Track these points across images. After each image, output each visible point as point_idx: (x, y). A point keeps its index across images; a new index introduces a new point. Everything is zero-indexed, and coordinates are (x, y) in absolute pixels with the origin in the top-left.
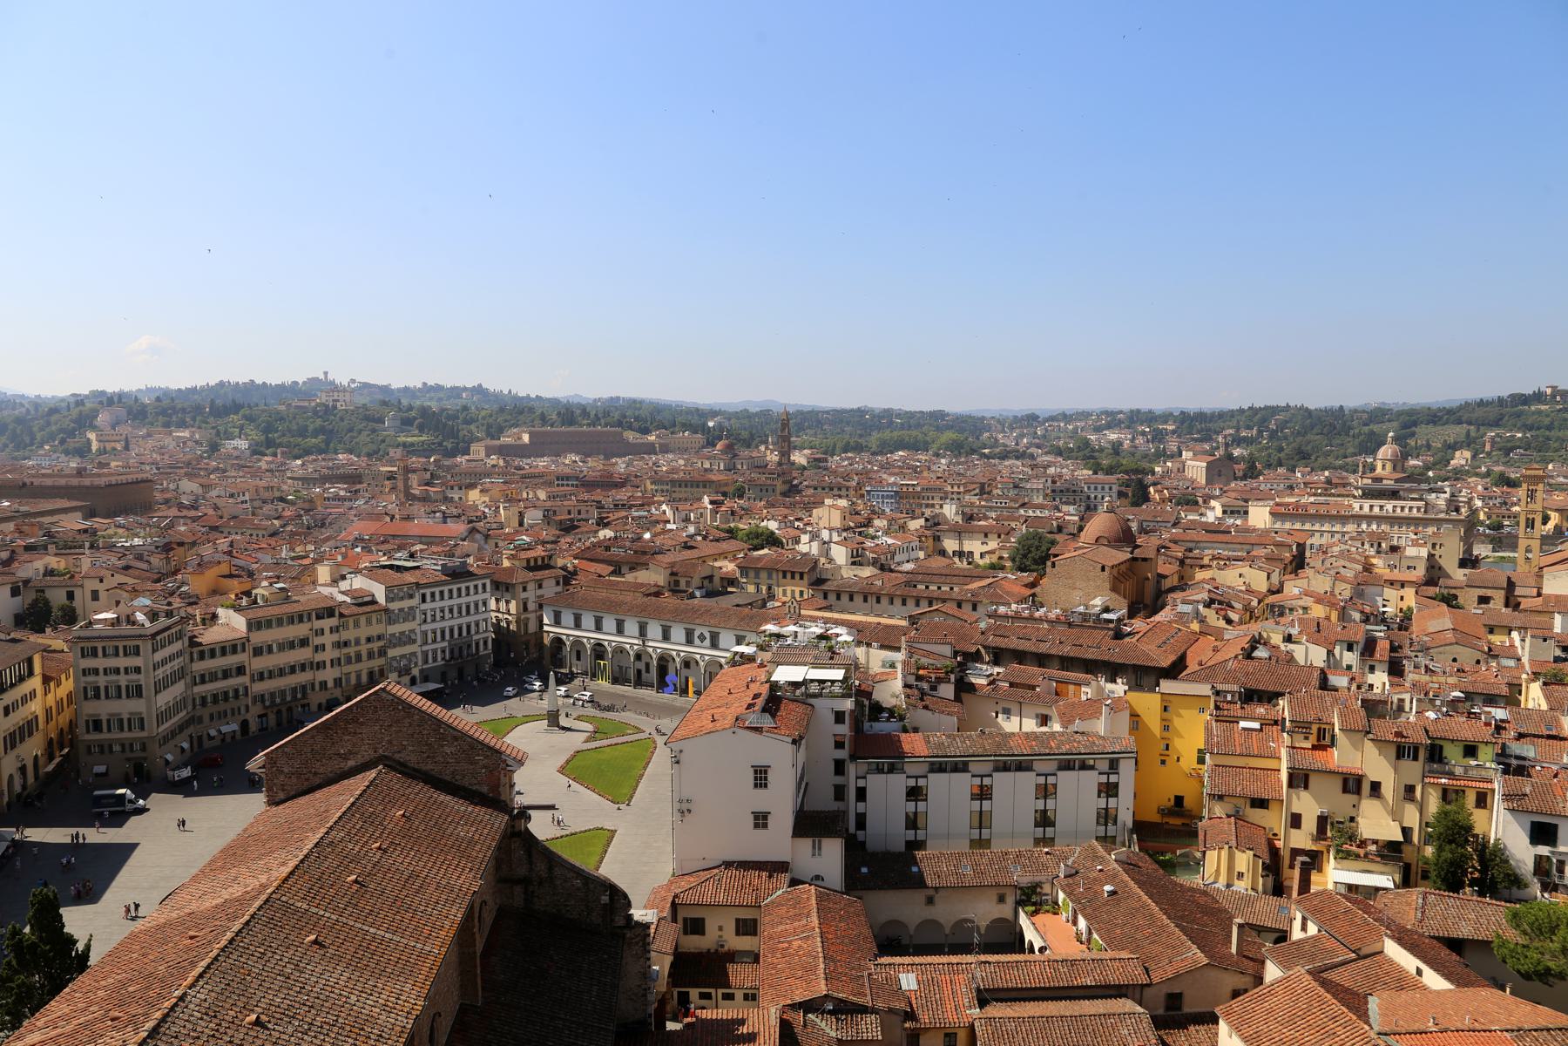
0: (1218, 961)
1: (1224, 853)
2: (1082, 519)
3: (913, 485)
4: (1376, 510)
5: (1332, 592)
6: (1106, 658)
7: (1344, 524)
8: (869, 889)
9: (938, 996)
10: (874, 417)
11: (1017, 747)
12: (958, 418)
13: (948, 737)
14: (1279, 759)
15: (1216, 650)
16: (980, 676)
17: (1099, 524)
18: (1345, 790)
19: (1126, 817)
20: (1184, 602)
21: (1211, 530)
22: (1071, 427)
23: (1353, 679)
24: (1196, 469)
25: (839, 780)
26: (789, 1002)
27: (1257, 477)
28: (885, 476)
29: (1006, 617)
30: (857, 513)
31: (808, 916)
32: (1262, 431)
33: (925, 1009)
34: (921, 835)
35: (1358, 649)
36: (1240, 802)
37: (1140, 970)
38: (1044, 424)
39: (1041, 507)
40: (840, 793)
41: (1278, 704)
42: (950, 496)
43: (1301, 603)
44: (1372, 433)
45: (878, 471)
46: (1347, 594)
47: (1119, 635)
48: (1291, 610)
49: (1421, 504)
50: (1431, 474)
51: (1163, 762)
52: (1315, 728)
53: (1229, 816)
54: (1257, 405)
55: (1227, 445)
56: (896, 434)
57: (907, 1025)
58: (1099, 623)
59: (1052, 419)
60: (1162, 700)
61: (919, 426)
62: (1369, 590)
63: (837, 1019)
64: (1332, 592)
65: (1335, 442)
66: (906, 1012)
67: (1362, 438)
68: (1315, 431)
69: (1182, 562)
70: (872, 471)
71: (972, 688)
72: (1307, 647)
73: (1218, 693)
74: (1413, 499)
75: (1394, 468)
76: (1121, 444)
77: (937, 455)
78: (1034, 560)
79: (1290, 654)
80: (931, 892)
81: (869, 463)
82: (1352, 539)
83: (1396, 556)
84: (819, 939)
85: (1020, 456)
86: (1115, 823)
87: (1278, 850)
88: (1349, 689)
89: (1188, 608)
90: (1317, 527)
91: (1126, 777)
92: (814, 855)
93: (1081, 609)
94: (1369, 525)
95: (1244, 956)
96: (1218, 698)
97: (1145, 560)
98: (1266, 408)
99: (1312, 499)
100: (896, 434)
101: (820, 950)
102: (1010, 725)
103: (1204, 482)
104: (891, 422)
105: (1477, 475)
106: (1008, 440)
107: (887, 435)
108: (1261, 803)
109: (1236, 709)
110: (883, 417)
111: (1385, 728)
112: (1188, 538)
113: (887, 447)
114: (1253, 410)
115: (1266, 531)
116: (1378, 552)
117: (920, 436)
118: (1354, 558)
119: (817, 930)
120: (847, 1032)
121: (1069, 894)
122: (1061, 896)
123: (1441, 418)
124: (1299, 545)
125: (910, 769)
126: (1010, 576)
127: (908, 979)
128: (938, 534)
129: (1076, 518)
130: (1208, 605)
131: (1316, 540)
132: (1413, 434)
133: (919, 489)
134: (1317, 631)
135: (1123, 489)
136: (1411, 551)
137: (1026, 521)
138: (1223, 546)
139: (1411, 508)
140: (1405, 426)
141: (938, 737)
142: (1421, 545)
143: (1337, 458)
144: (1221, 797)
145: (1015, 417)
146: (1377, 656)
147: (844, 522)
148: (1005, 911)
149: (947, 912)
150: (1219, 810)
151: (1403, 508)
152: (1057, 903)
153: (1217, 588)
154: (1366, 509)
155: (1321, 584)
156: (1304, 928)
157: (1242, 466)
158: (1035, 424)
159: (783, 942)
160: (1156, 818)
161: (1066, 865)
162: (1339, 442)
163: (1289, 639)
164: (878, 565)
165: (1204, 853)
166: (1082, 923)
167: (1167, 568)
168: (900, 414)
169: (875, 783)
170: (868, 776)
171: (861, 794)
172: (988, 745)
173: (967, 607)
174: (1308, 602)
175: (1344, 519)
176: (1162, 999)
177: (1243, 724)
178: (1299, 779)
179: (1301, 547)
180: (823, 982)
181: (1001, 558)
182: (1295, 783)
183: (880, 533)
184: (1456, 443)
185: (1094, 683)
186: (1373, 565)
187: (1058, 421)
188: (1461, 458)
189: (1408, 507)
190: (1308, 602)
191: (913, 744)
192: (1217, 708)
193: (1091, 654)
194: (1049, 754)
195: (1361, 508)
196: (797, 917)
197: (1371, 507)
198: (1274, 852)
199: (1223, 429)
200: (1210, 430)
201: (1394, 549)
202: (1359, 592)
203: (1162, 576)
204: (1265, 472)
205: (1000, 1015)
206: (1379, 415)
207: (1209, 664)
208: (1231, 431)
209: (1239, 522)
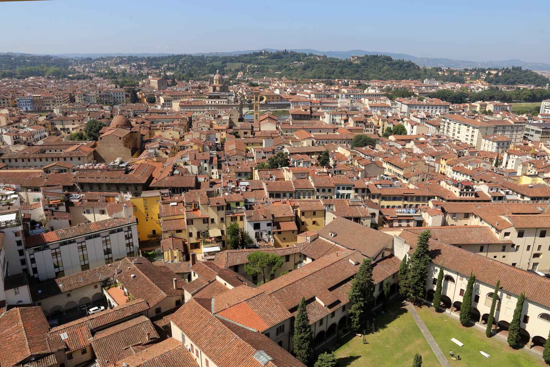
0: (170, 294)
1: (170, 252)
2: (111, 112)
3: (39, 96)
4: (213, 103)
5: (200, 138)
6: (123, 182)
7: (203, 109)
8: (43, 299)
9: (76, 338)
10: (16, 59)
11: (93, 229)
12: (56, 60)
13: (66, 230)
14: (184, 215)
15: (161, 172)
16: (75, 198)
17: (117, 120)
18: (204, 223)
19: (136, 244)
20: (151, 149)
21: (159, 113)
22: (106, 63)
23: (205, 178)
24: (154, 82)
25: (22, 257)
26: (15, 363)
27: (176, 85)
28: (25, 91)
29: (83, 170)
30: (13, 116)
31: (18, 321)
32: (177, 65)
33: (72, 344)
34: (61, 269)
35: (208, 162)
36: (173, 232)
37: (146, 304)
38: (94, 62)
39: (95, 107)
40: (23, 262)
41: (182, 195)
42: (56, 100)
43: (190, 145)
44: (213, 66)
45: (21, 88)
46: (204, 139)
47: (127, 172)
48: (187, 147)
49: (226, 100)
50: (231, 81)
51: (147, 220)
52: (193, 204)
53: (170, 237)
54: (175, 55)
55: (165, 71)
56: (28, 68)
57: (66, 353)
58: (119, 168)
59: (98, 60)
60: (144, 200)
61: (39, 63)
62: (212, 136)
63: (37, 362)
64: (200, 138)
65: (201, 69)
66: (65, 349)
67: (210, 67)
68: (195, 65)
69: (150, 128)
70: (18, 88)
71: (72, 204)
72: (191, 167)
73: (162, 194)
74: (224, 99)
75: (219, 83)
76: (126, 71)
77: (49, 78)
78: (94, 131)
79: (187, 169)
80: (69, 292)
81: (17, 84)
82: (206, 114)
83: (220, 119)
84: (24, 332)
85: (85, 78)
86: (133, 246)
87: (186, 244)
88: (205, 182)
89: (152, 151)
90: (195, 110)
91: (134, 231)
92: (16, 293)
93: (111, 164)
94: (211, 108)
95: (178, 289)
96: (163, 196)
97: (135, 132)
98: (178, 56)
99: (193, 100)
100: (28, 68)
101: (25, 336)
102: (90, 217)
103: (157, 88)
104: (25, 62)
105: (245, 81)
106: (79, 69)
107: (24, 69)
108: (180, 231)
109: (168, 199)
110: (21, 59)
111: (214, 200)
112: (151, 118)
113: (24, 75)
114: (174, 57)
115: (178, 112)
116: (215, 118)
117: (40, 69)
118: (207, 122)
119: (23, 327)
120: (42, 365)
121: (120, 280)
122: (117, 281)
123: (234, 60)
124: (189, 118)
125: (51, 247)
126: (84, 143)
127: (64, 335)
128: (53, 122)
129: (109, 112)
130: (159, 149)
131: (195, 114)
132: (226, 66)
133: (42, 98)
134: (195, 160)
135: (127, 93)
136: (224, 118)
137: (90, 114)
138: (164, 120)
139: (224, 102)
140: (223, 63)
141: (61, 231)
142: (227, 115)
143: (202, 75)
144: (167, 232)
145: (82, 59)
146: (214, 163)
147: (8, 121)
148: (98, 290)
149: (76, 298)
150: (167, 235)
151: (221, 102)
152: (116, 283)
153: (162, 141)
154: (210, 103)
155: (196, 135)
156: (194, 275)
157: (170, 80)
158: (91, 62)
159: (8, 337)
160: (147, 239)
161: (117, 270)
162: (203, 69)
163: (185, 164)
164: (27, 144)
165: (163, 253)
166: (126, 290)
167: (144, 131)
168: (29, 58)
169: (38, 255)
170: (34, 253)
171: (33, 261)
172: (82, 230)
173: (68, 160)
174: (192, 144)
175: (203, 106)
176: (154, 312)
177: (171, 204)
178: (190, 222)
179: (190, 119)
180: (29, 350)
181: (81, 130)
182: (189, 223)
183: (26, 126)
184: (238, 69)
185: (119, 195)
186: (212, 123)
187: (100, 60)
188: (240, 75)
189: (223, 102)
190: (192, 144)
191: (50, 237)
192: (162, 199)
193: (117, 181)
194: (105, 229)
195: (208, 102)
196: (13, 323)
197: (212, 102)
198: (185, 246)
199: (163, 64)
200: (158, 65)
201: (219, 116)
202: (208, 138)
203: (143, 135)
204: (178, 82)
205: (100, 337)
206: (215, 58)
207: (160, 179)
208: (166, 65)
209: (169, 109)
